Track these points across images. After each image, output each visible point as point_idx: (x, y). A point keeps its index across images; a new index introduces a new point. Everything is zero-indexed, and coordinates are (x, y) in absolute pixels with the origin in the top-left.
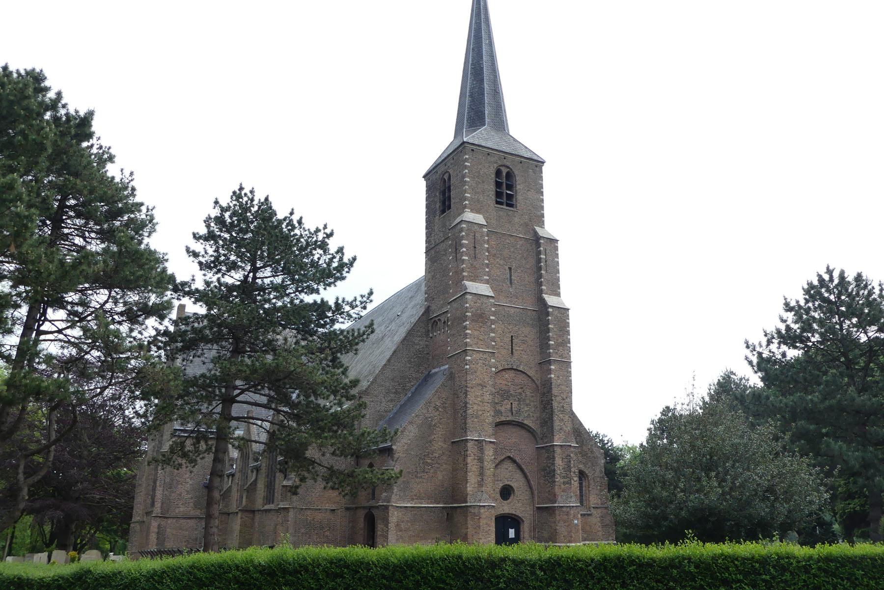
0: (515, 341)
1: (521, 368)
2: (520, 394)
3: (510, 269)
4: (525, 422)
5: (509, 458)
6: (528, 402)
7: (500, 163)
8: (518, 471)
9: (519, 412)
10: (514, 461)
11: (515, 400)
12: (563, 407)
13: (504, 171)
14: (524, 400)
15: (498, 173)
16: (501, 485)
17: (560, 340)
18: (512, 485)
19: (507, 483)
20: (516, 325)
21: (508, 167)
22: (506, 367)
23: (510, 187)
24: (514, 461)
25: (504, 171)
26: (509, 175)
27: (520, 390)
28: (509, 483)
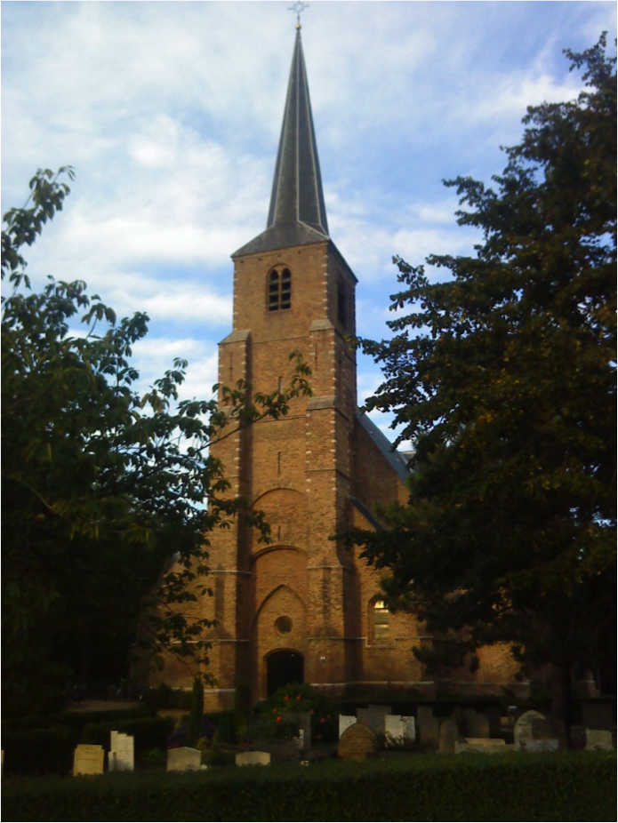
0: (283, 457)
1: (290, 486)
2: (291, 514)
3: (280, 378)
4: (296, 545)
5: (281, 586)
6: (299, 522)
7: (272, 264)
8: (296, 600)
9: (288, 535)
10: (290, 591)
11: (283, 523)
12: (322, 524)
13: (280, 270)
14: (295, 521)
15: (274, 275)
16: (277, 617)
17: (320, 447)
18: (290, 616)
19: (283, 614)
20: (284, 439)
21: (283, 264)
22: (273, 488)
23: (287, 286)
24: (290, 591)
25: (280, 270)
26: (287, 273)
27: (291, 511)
28: (285, 614)
